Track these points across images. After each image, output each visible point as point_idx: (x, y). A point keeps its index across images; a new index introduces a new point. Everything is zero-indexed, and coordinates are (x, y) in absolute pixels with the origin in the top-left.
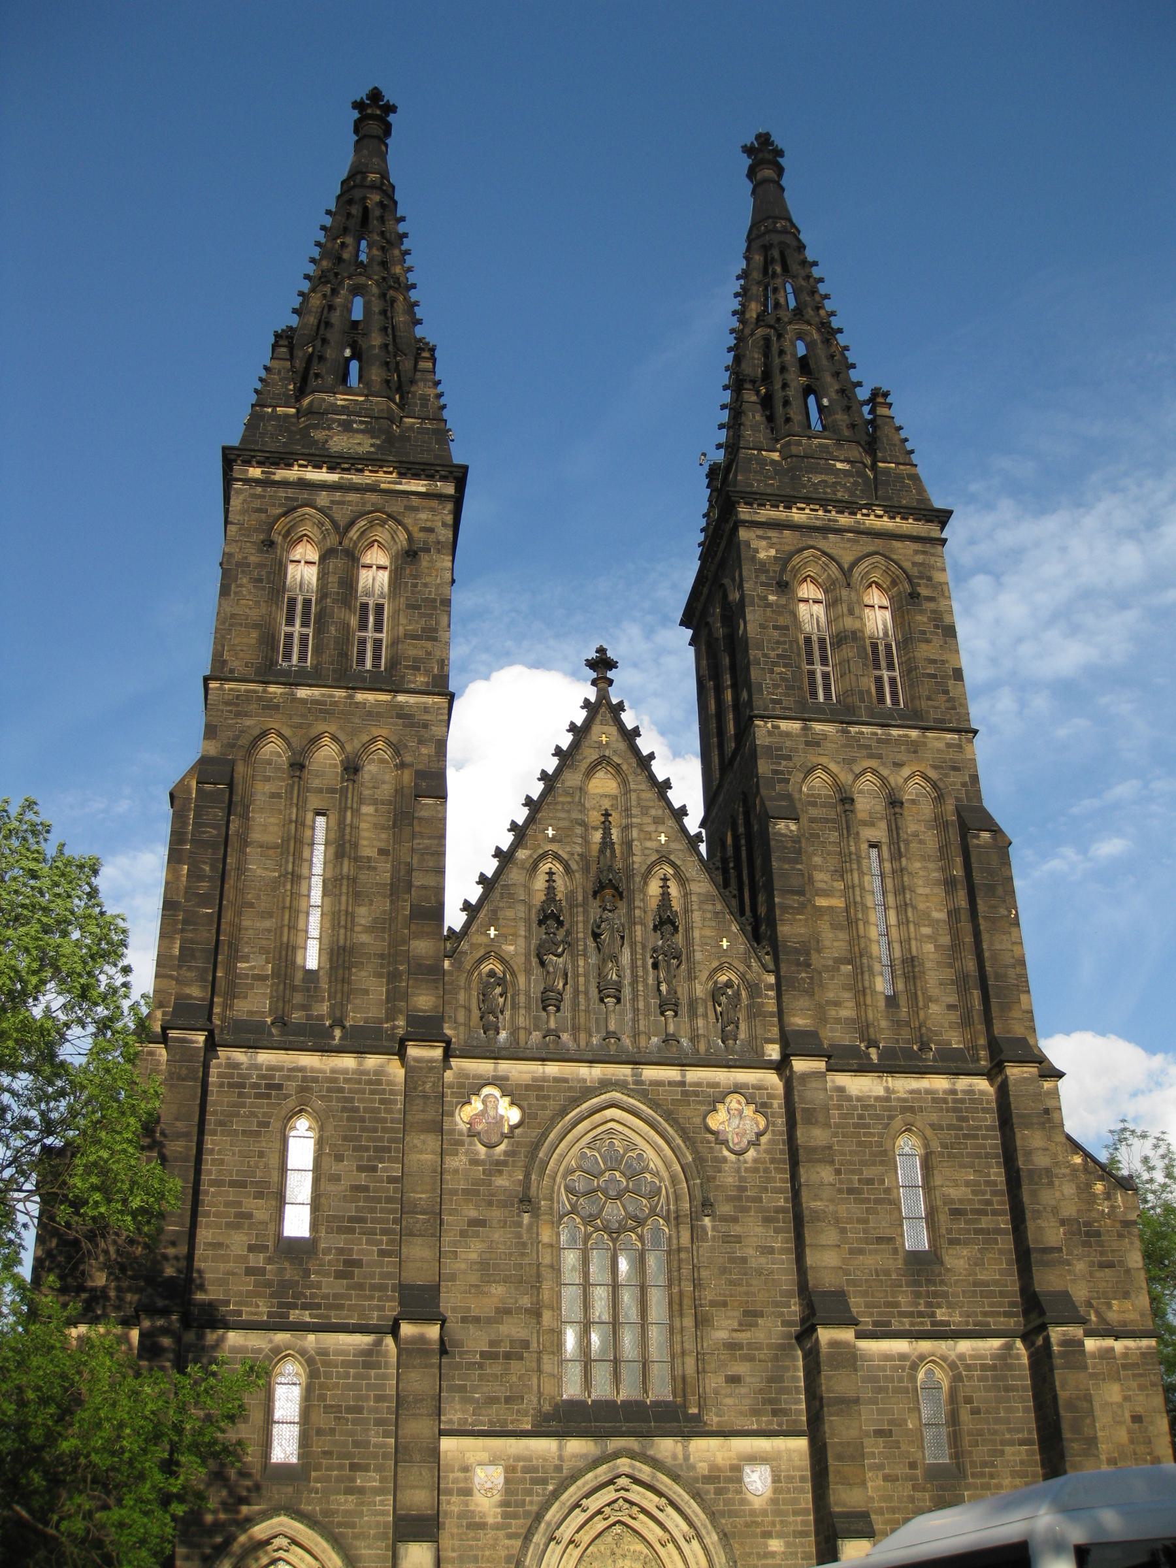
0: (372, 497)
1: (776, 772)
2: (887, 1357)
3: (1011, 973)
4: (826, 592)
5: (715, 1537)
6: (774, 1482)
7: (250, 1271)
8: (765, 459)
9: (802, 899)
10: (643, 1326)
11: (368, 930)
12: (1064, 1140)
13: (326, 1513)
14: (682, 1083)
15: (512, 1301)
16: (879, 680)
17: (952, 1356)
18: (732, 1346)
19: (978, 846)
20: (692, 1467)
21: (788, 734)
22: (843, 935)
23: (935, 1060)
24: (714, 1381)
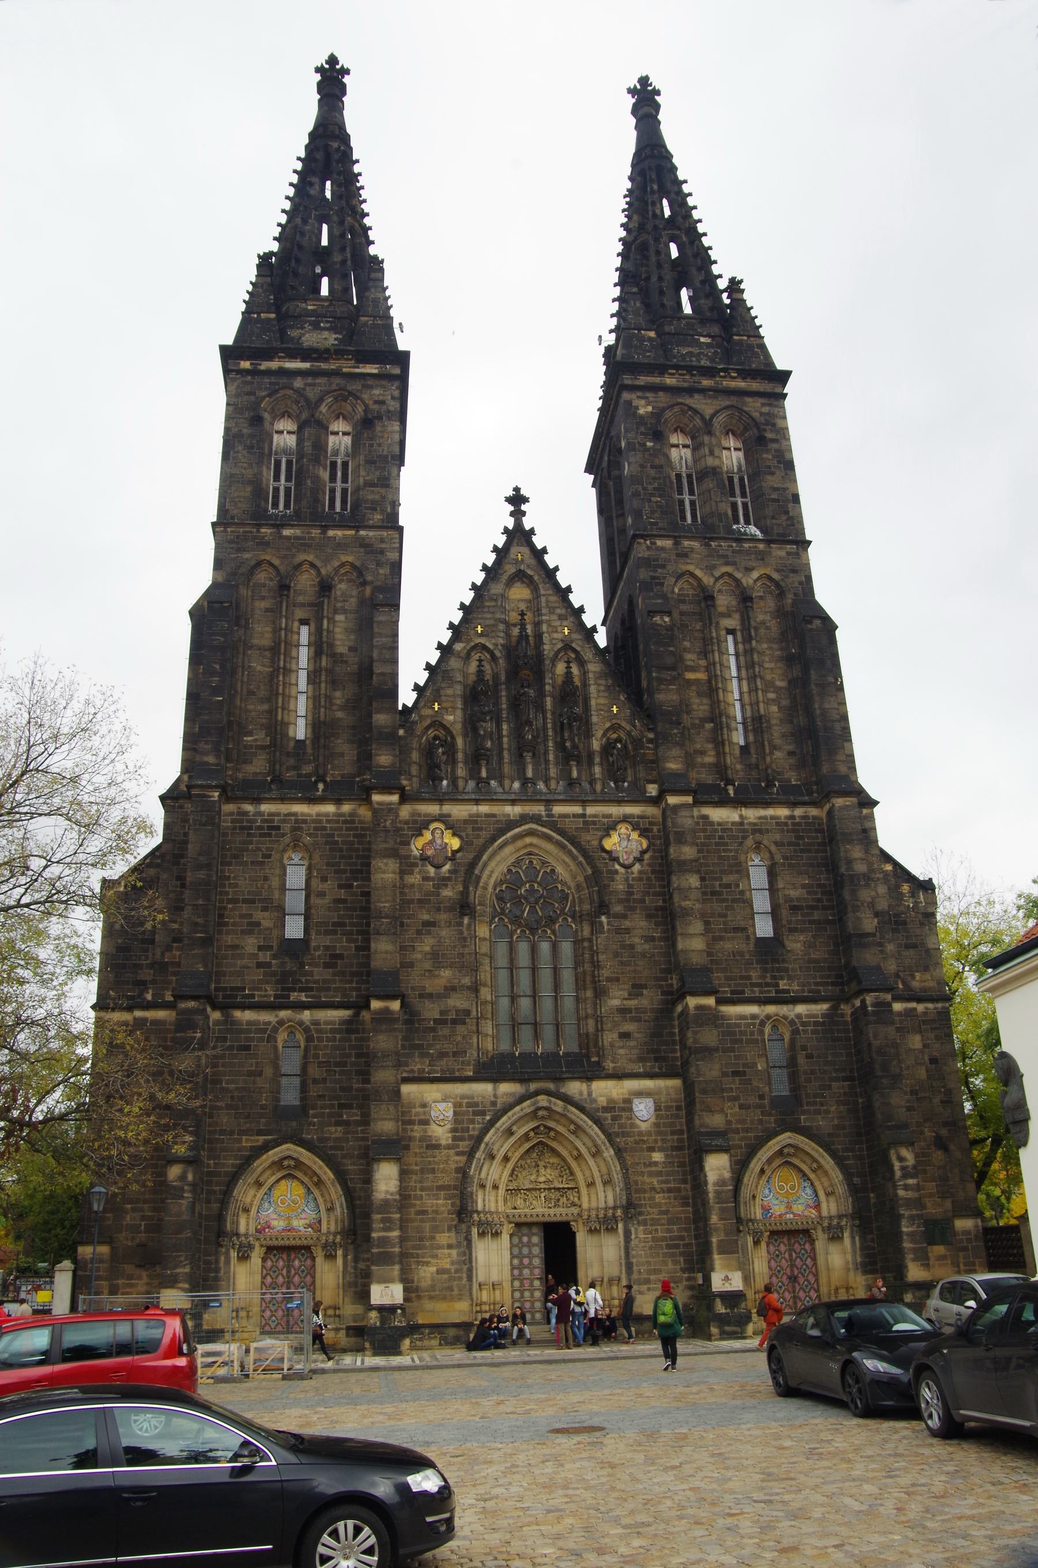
0: (337, 381)
1: (653, 578)
2: (743, 1017)
3: (838, 726)
4: (693, 438)
5: (612, 1152)
6: (656, 1110)
7: (259, 965)
8: (643, 336)
9: (674, 673)
10: (556, 997)
11: (342, 708)
12: (878, 852)
13: (321, 1140)
14: (584, 815)
16: (734, 506)
18: (623, 1011)
19: (811, 630)
20: (595, 1101)
21: (663, 549)
22: (705, 701)
23: (778, 793)
24: (609, 1037)
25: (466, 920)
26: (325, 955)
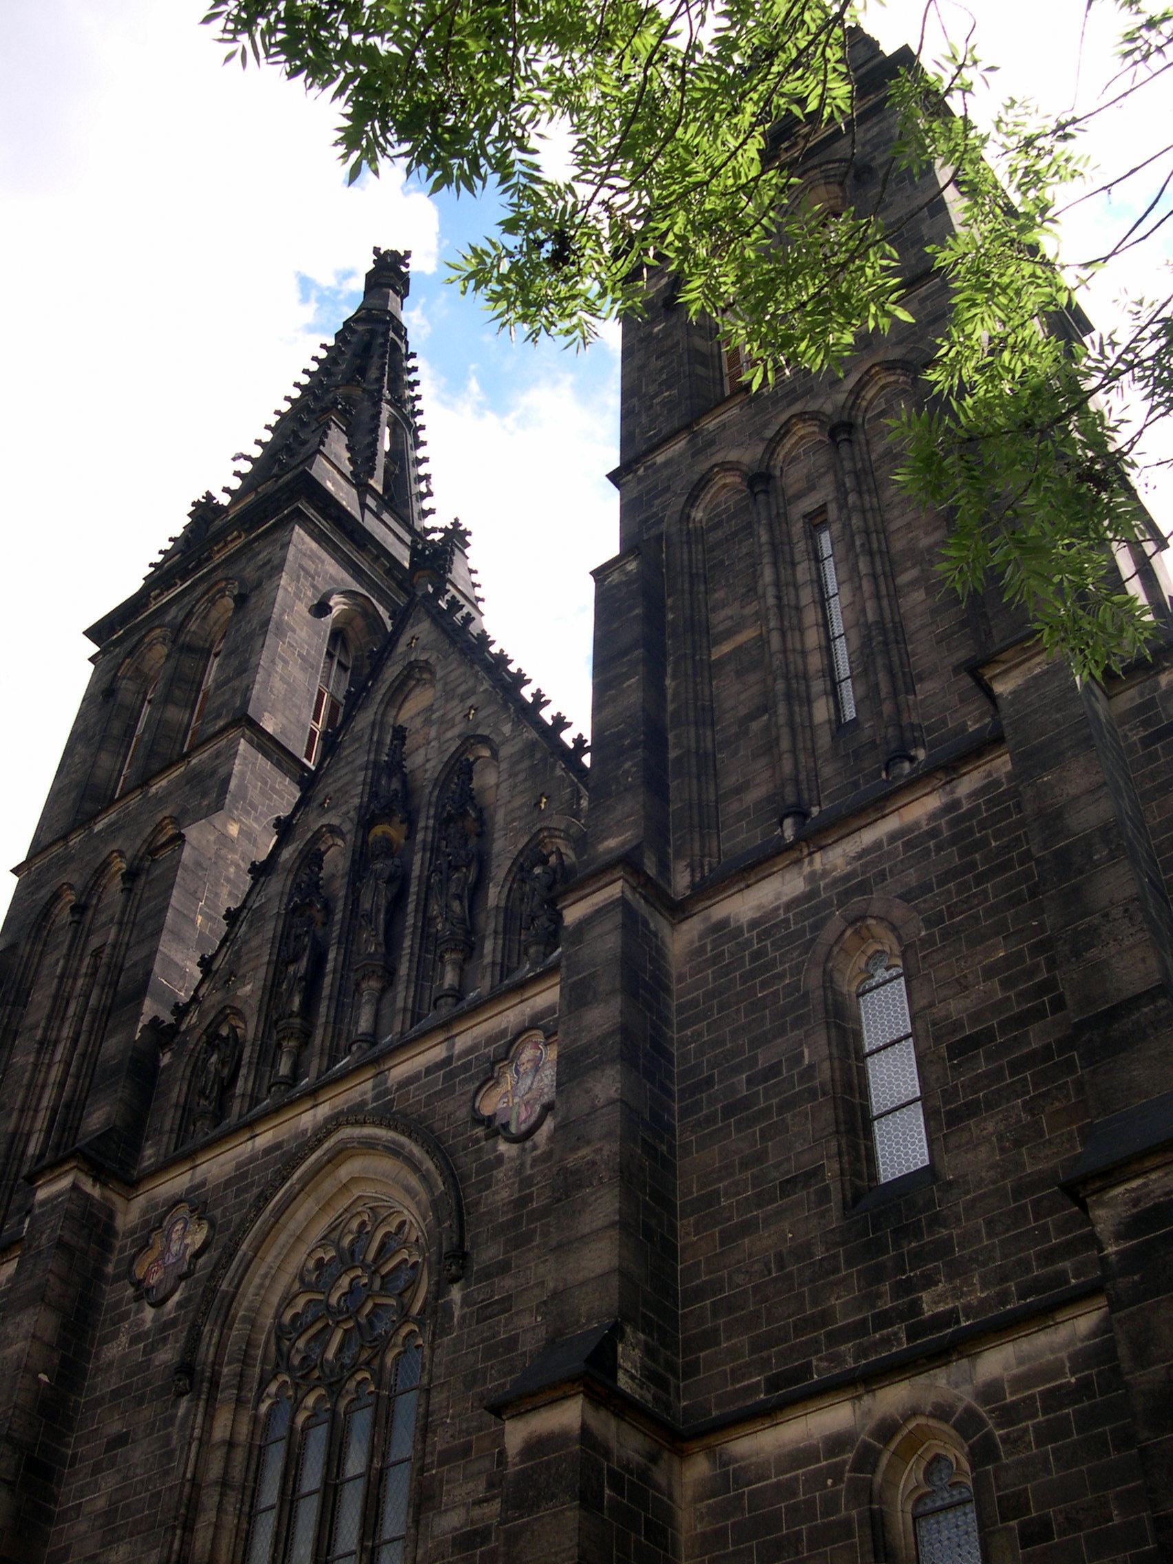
14: (448, 1060)
17: (965, 1396)
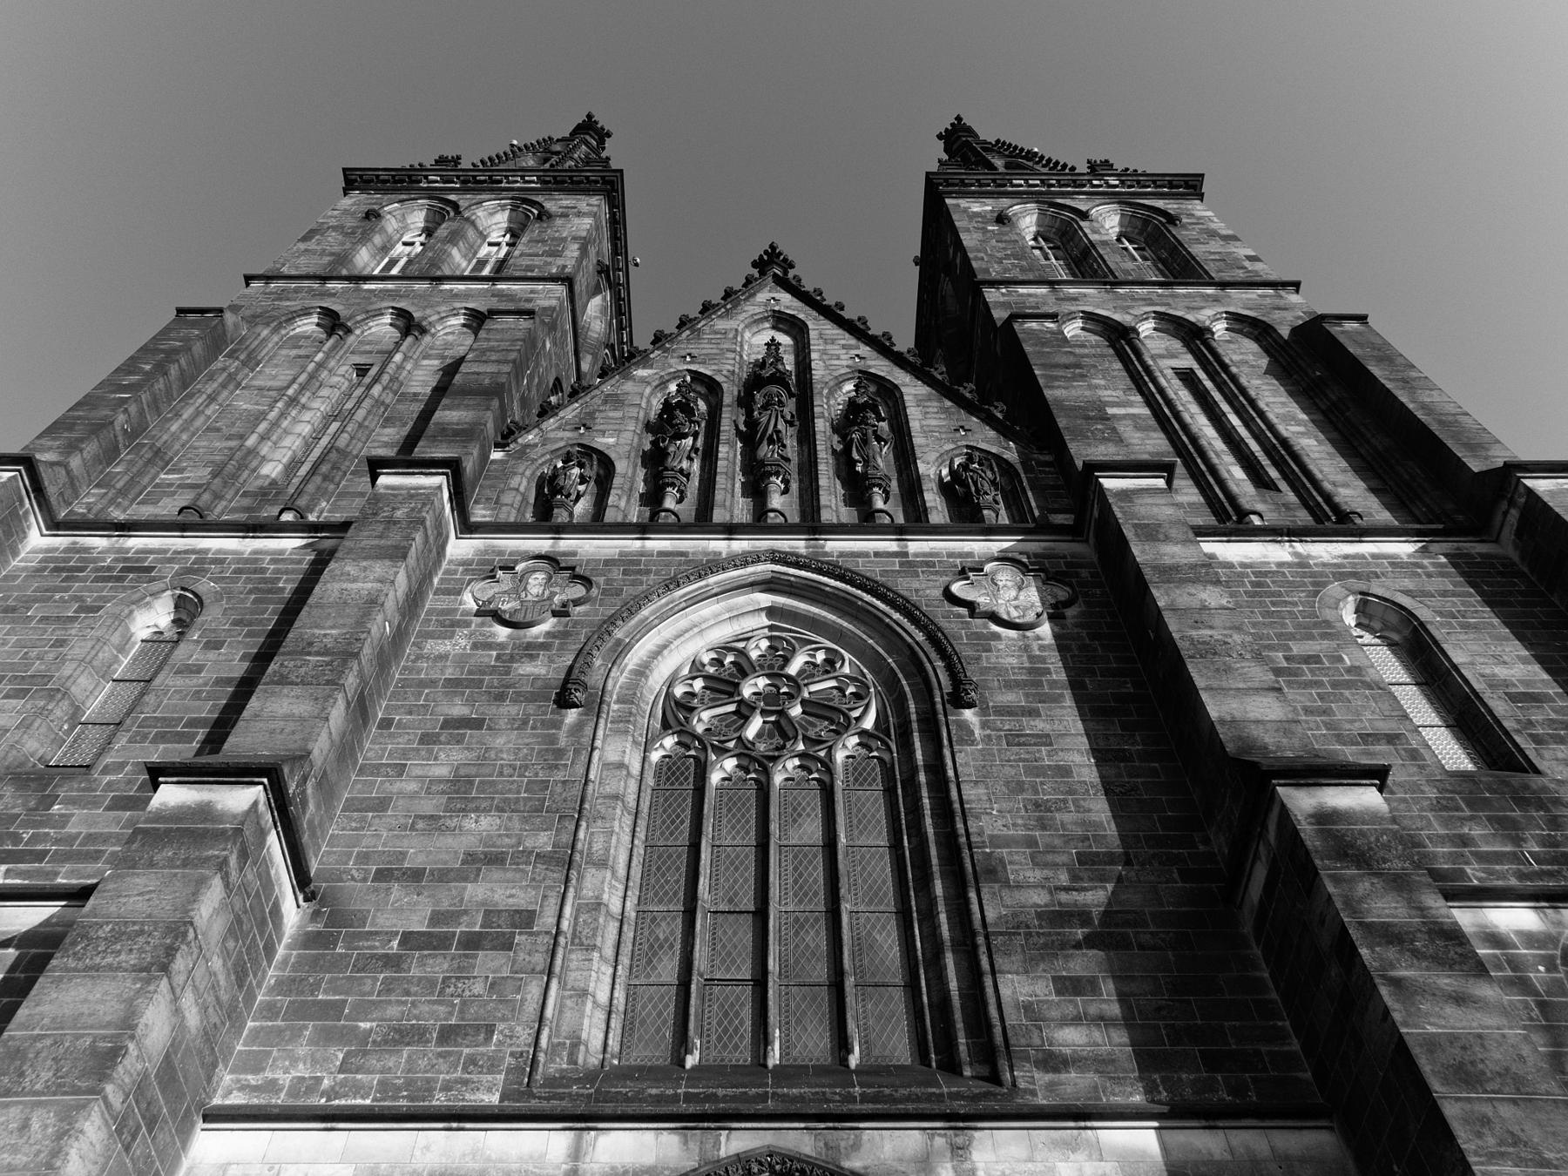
15: (514, 841)
25: (572, 715)
26: (129, 782)
